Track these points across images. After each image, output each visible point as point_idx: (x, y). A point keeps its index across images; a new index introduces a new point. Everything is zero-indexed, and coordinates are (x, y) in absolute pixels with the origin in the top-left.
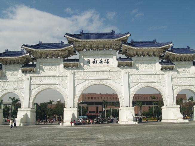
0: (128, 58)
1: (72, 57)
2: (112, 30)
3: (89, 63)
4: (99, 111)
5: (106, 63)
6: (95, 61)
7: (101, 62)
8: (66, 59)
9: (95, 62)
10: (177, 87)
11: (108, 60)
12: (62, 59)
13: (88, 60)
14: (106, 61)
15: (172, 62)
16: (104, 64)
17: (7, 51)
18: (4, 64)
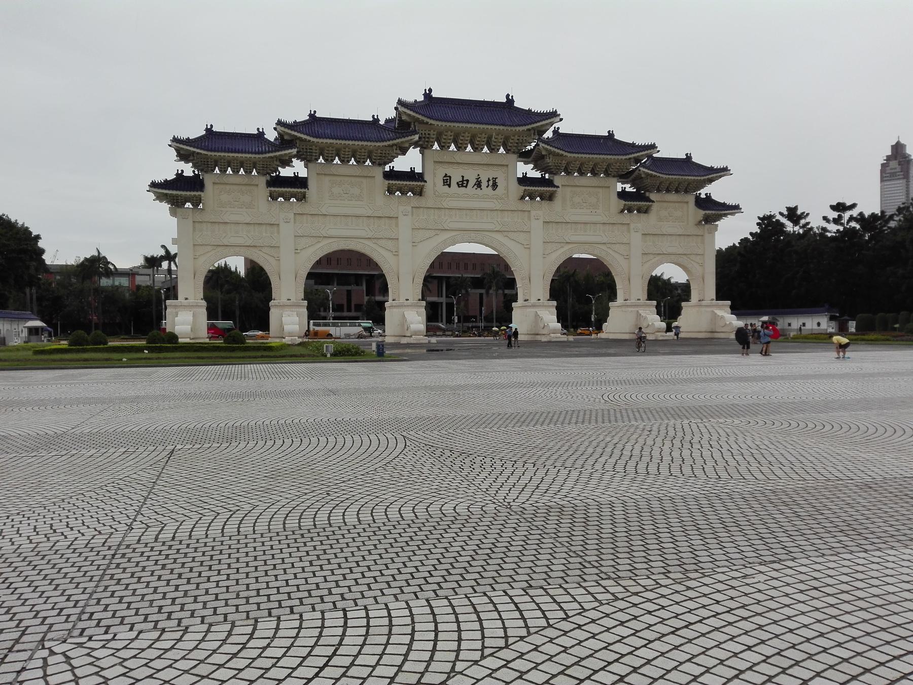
0: (543, 177)
1: (401, 164)
2: (508, 96)
3: (449, 186)
4: (355, 305)
5: (490, 188)
6: (463, 180)
7: (478, 184)
8: (387, 168)
9: (463, 183)
10: (652, 256)
11: (495, 179)
12: (378, 172)
13: (446, 175)
14: (491, 183)
15: (647, 194)
16: (486, 191)
17: (209, 131)
18: (206, 172)
